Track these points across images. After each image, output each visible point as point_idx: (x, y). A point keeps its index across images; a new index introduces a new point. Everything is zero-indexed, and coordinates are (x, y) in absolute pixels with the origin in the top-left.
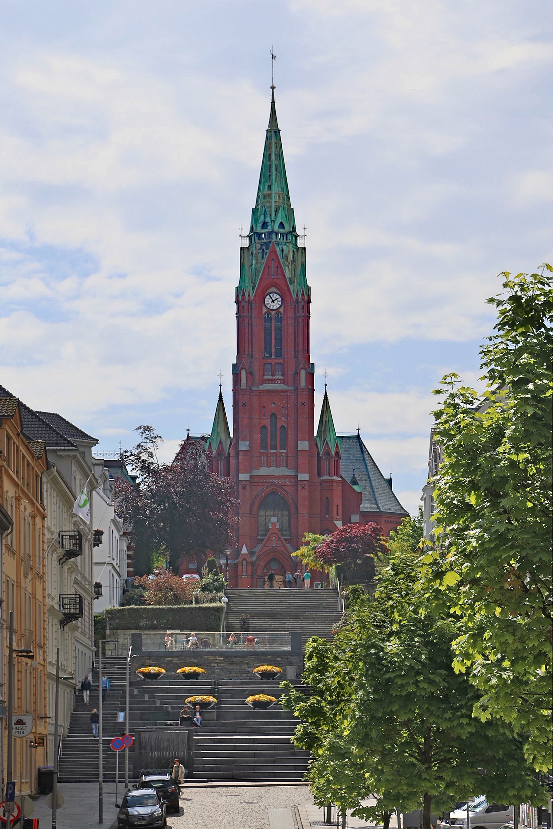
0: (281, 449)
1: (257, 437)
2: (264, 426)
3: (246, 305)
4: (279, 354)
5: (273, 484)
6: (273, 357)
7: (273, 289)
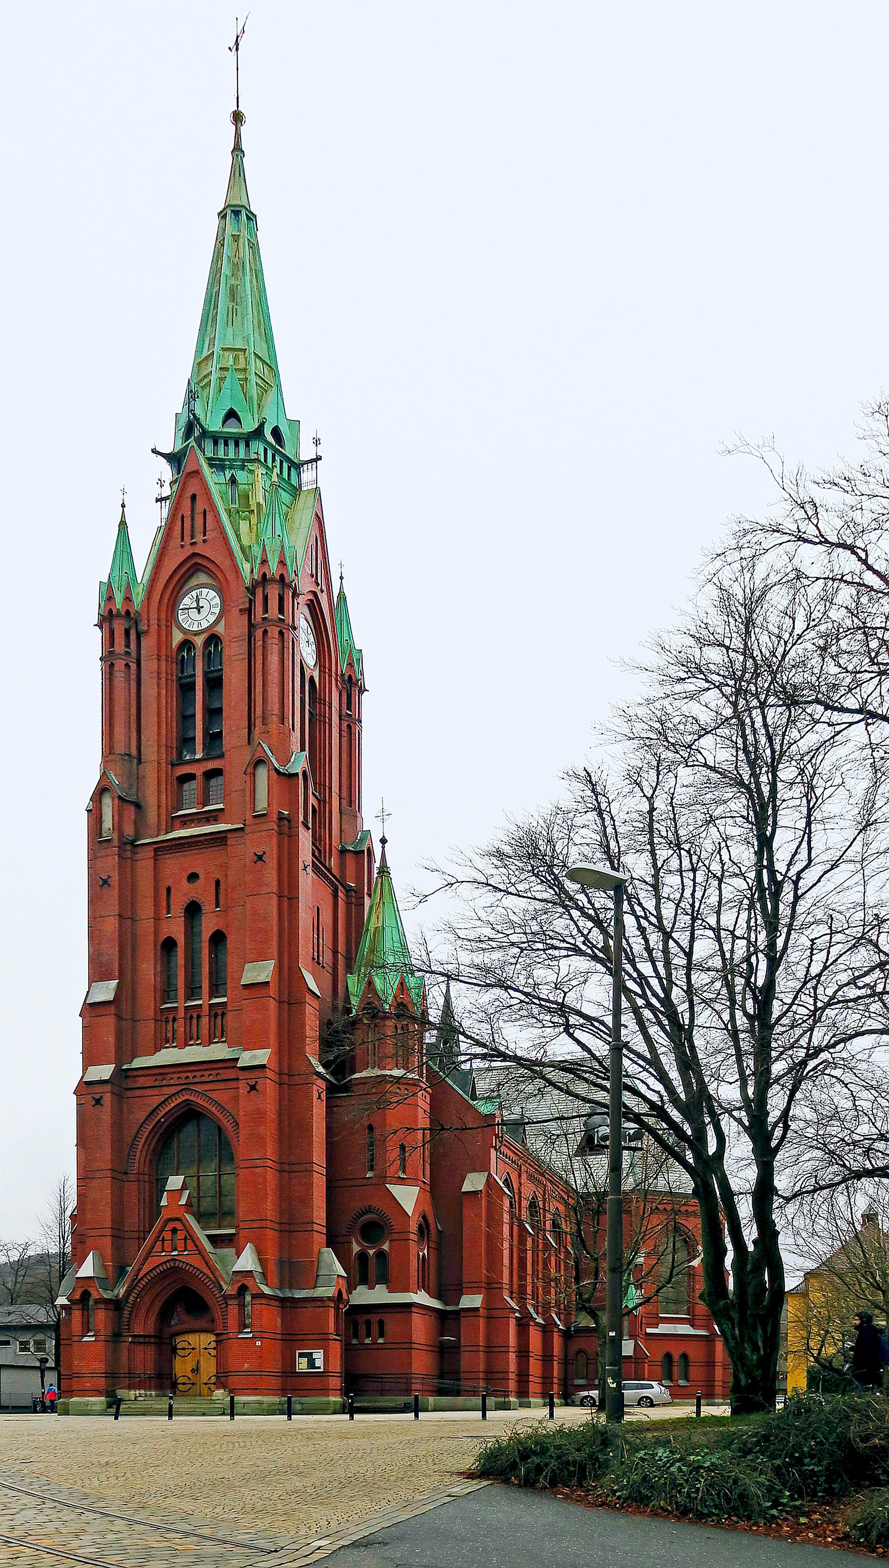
3: (122, 625)
7: (202, 578)
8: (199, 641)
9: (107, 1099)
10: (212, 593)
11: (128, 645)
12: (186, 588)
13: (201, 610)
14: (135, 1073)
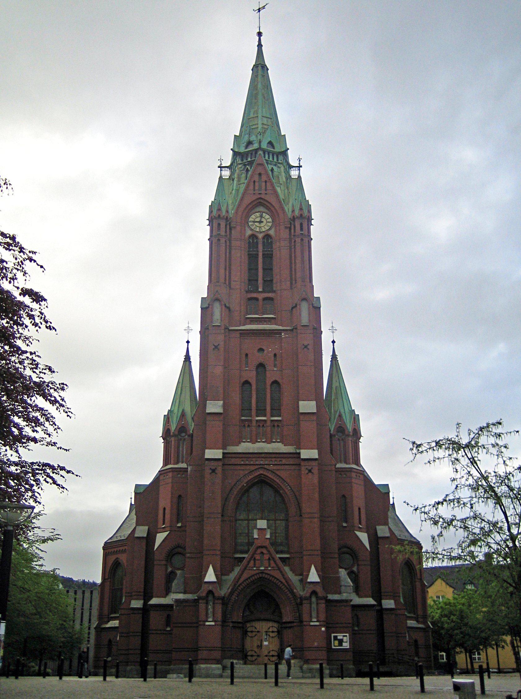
0: (272, 416)
1: (236, 397)
2: (247, 382)
3: (222, 224)
4: (269, 283)
5: (262, 467)
6: (260, 290)
7: (262, 209)
8: (260, 236)
9: (219, 469)
10: (267, 217)
11: (226, 232)
12: (253, 211)
13: (261, 223)
14: (229, 455)
